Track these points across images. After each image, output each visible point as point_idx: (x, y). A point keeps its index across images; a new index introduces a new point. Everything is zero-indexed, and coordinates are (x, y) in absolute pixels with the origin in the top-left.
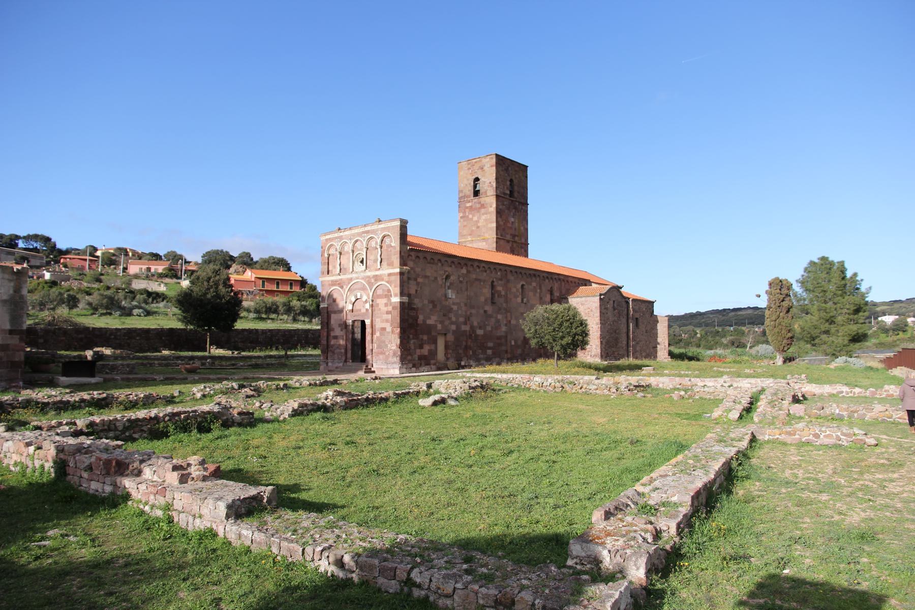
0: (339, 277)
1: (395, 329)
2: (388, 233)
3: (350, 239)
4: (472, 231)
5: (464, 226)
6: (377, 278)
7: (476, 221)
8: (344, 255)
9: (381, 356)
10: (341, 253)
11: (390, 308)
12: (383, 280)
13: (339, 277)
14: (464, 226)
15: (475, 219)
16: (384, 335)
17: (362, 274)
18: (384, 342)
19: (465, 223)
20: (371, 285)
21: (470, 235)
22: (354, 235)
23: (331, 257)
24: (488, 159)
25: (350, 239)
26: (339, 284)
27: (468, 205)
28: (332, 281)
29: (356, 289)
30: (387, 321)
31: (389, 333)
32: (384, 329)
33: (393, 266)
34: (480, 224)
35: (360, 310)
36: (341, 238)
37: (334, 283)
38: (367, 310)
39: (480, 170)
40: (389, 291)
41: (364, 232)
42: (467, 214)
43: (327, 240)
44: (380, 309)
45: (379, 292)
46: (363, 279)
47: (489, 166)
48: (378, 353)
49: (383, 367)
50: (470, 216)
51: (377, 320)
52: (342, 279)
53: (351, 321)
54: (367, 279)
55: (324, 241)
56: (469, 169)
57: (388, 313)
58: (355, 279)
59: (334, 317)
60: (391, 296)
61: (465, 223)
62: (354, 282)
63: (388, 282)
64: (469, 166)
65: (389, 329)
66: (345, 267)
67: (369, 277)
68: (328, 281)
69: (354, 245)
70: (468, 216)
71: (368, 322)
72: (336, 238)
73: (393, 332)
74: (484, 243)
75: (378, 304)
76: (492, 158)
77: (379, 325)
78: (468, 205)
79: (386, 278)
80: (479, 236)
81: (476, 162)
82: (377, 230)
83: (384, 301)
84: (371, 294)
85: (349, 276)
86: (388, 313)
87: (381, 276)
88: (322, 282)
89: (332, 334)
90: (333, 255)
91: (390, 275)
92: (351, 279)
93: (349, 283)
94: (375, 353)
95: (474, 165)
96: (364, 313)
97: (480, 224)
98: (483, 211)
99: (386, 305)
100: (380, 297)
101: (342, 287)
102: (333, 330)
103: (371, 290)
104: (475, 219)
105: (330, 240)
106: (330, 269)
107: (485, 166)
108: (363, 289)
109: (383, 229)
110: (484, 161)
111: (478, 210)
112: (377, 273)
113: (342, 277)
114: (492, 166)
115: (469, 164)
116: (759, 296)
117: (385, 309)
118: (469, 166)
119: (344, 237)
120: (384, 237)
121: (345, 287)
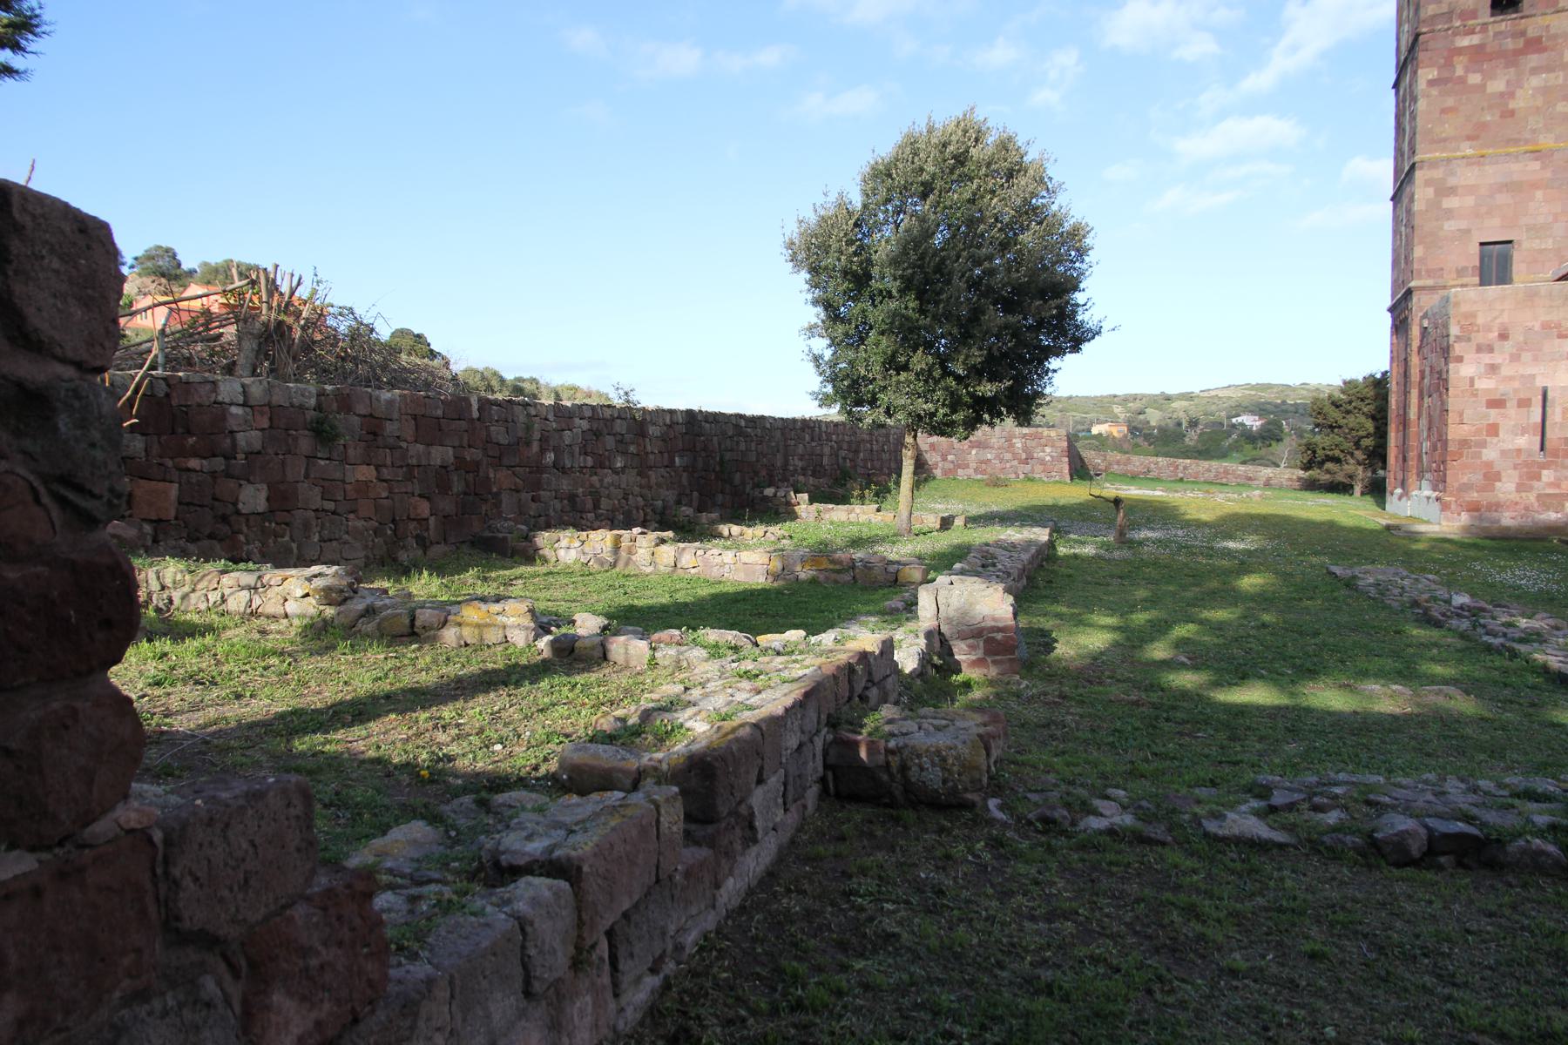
4: (1483, 126)
5: (1444, 111)
7: (1502, 95)
14: (1444, 111)
15: (1497, 86)
19: (1450, 102)
21: (1469, 138)
27: (1465, 42)
34: (1517, 104)
42: (1459, 71)
50: (1474, 79)
61: (1450, 102)
70: (1462, 80)
74: (1537, 165)
78: (1465, 42)
80: (1516, 142)
97: (1517, 104)
98: (1533, 60)
104: (1497, 86)
111: (1512, 58)
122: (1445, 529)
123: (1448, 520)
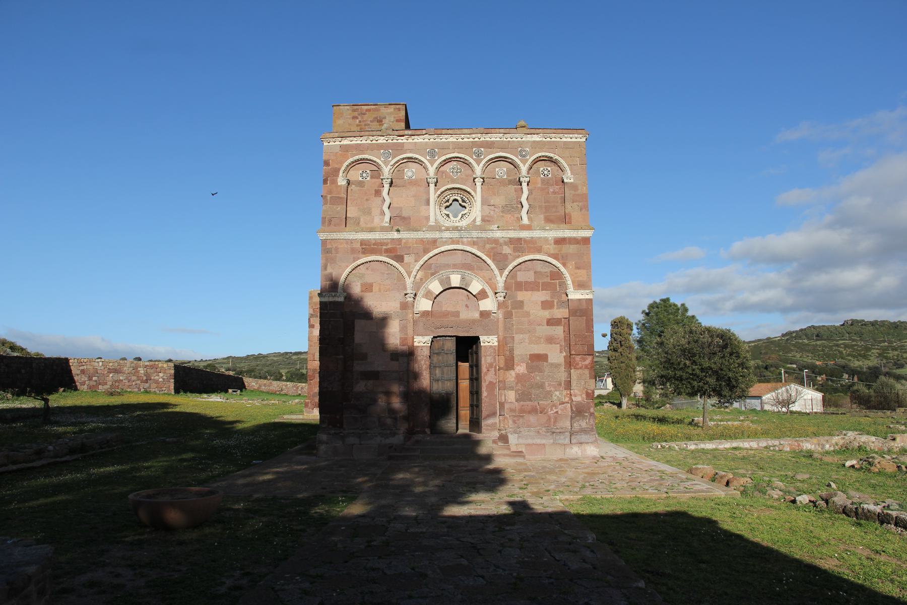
0: (395, 235)
1: (578, 358)
2: (551, 155)
3: (432, 154)
6: (518, 245)
8: (396, 186)
9: (532, 419)
10: (391, 184)
11: (561, 313)
12: (539, 250)
13: (395, 235)
16: (541, 371)
17: (475, 234)
18: (541, 386)
20: (501, 261)
22: (444, 147)
23: (353, 187)
24: (391, 109)
25: (432, 154)
26: (387, 251)
28: (363, 242)
29: (446, 266)
30: (550, 340)
31: (557, 366)
32: (543, 358)
33: (570, 223)
35: (457, 314)
36: (399, 148)
37: (368, 248)
38: (485, 314)
39: (376, 123)
40: (557, 275)
41: (474, 144)
43: (346, 149)
44: (528, 314)
45: (521, 277)
46: (474, 244)
47: (392, 119)
48: (522, 411)
49: (543, 441)
51: (518, 337)
52: (400, 240)
53: (428, 338)
54: (488, 246)
55: (338, 150)
56: (355, 118)
57: (551, 322)
58: (445, 243)
59: (359, 324)
60: (563, 285)
62: (443, 249)
63: (555, 257)
64: (356, 114)
65: (556, 356)
66: (405, 214)
67: (496, 241)
68: (352, 241)
69: (438, 169)
71: (488, 341)
72: (380, 146)
73: (569, 364)
75: (522, 302)
76: (399, 109)
77: (523, 348)
79: (552, 248)
81: (369, 110)
82: (521, 144)
83: (542, 296)
84: (500, 281)
85: (429, 235)
86: (551, 322)
87: (532, 241)
88: (324, 242)
89: (358, 367)
90: (361, 184)
91: (560, 241)
92: (434, 243)
93: (426, 251)
94: (512, 410)
95: (364, 114)
96: (474, 321)
99: (546, 305)
100: (520, 286)
101: (400, 259)
102: (364, 357)
103: (502, 270)
105: (359, 148)
106: (348, 215)
107: (385, 118)
108: (473, 264)
109: (536, 145)
110: (384, 111)
112: (524, 234)
113: (404, 235)
114: (398, 121)
115: (354, 111)
116: (604, 336)
117: (546, 314)
118: (356, 114)
119: (406, 147)
120: (536, 162)
121: (407, 259)
122: (305, 417)
123: (307, 413)
